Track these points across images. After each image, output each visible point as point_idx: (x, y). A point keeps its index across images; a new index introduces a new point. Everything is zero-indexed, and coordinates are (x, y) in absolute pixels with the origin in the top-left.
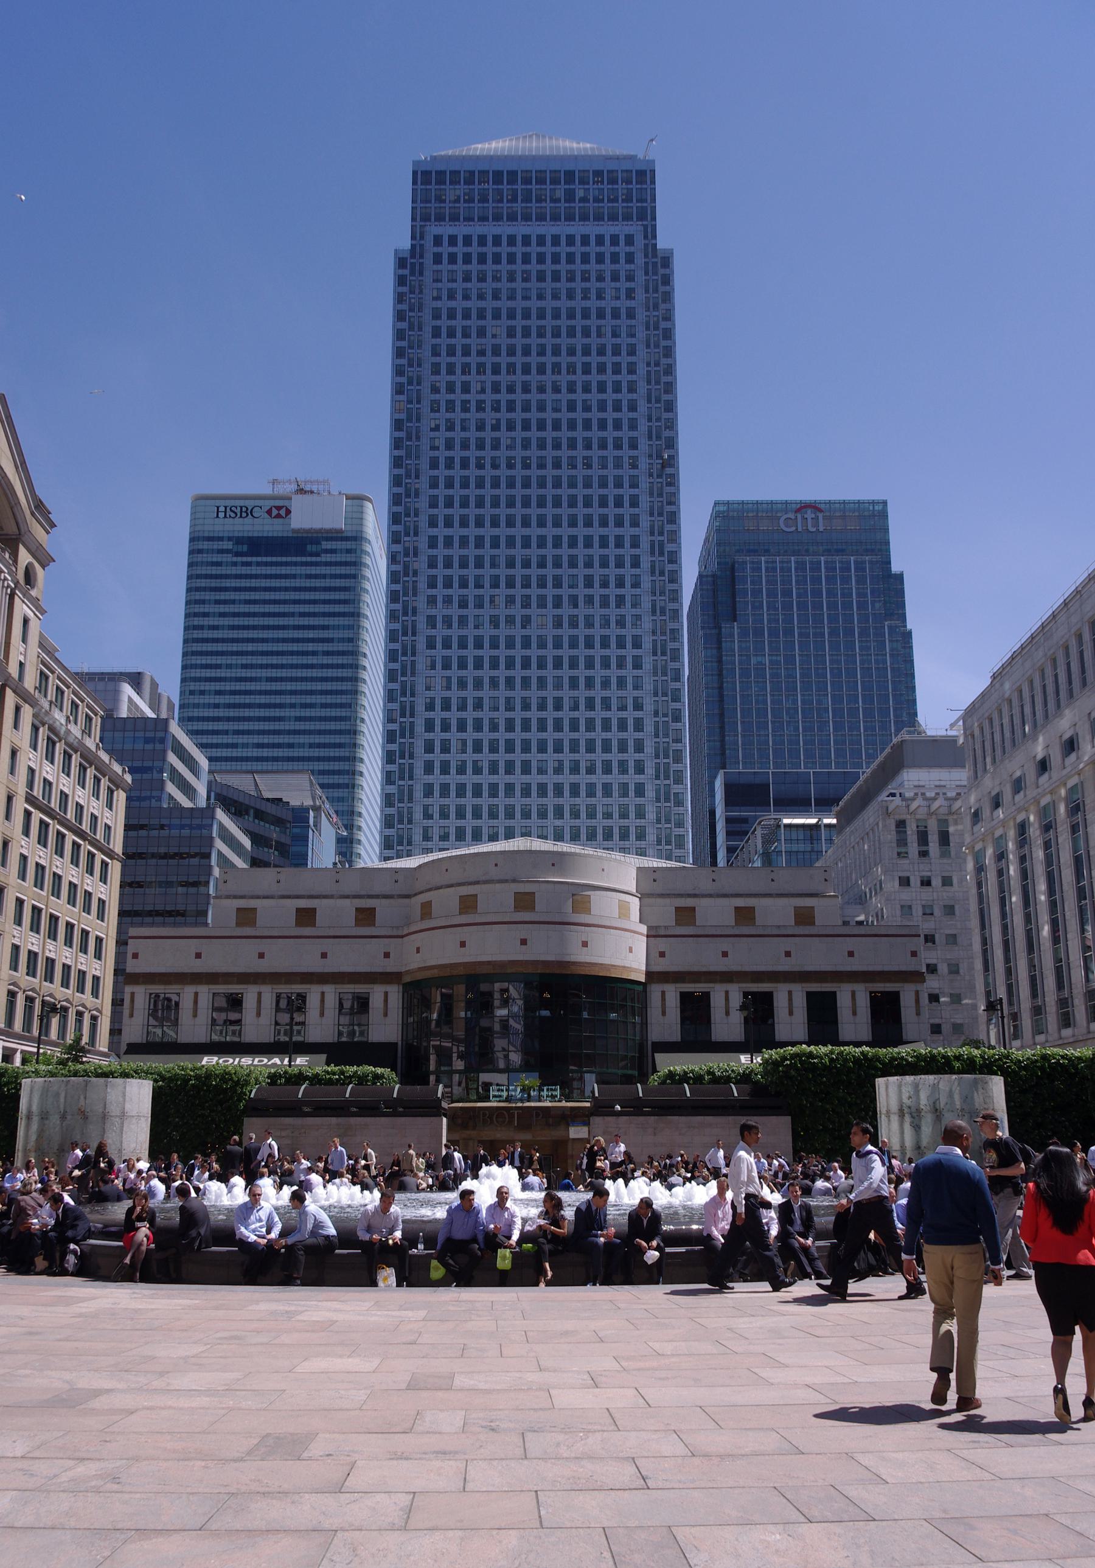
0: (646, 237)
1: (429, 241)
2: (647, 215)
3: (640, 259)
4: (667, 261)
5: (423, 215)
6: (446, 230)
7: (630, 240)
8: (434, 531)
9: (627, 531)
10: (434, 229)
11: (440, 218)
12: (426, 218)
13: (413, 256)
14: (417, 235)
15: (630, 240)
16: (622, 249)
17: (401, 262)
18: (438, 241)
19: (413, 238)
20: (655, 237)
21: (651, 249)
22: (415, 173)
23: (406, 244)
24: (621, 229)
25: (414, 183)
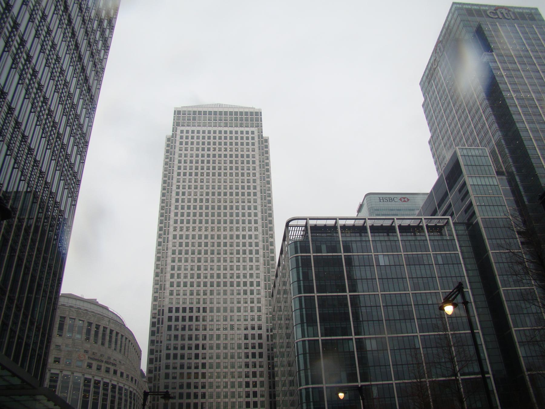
0: (259, 132)
1: (178, 132)
2: (259, 126)
3: (256, 139)
4: (266, 141)
5: (176, 124)
6: (185, 129)
7: (253, 133)
8: (175, 233)
9: (253, 233)
10: (180, 129)
11: (183, 126)
12: (178, 125)
13: (172, 137)
14: (174, 130)
15: (253, 133)
16: (250, 135)
17: (168, 140)
18: (182, 132)
19: (173, 131)
20: (262, 132)
21: (260, 136)
22: (175, 111)
23: (170, 133)
24: (250, 129)
25: (175, 114)
